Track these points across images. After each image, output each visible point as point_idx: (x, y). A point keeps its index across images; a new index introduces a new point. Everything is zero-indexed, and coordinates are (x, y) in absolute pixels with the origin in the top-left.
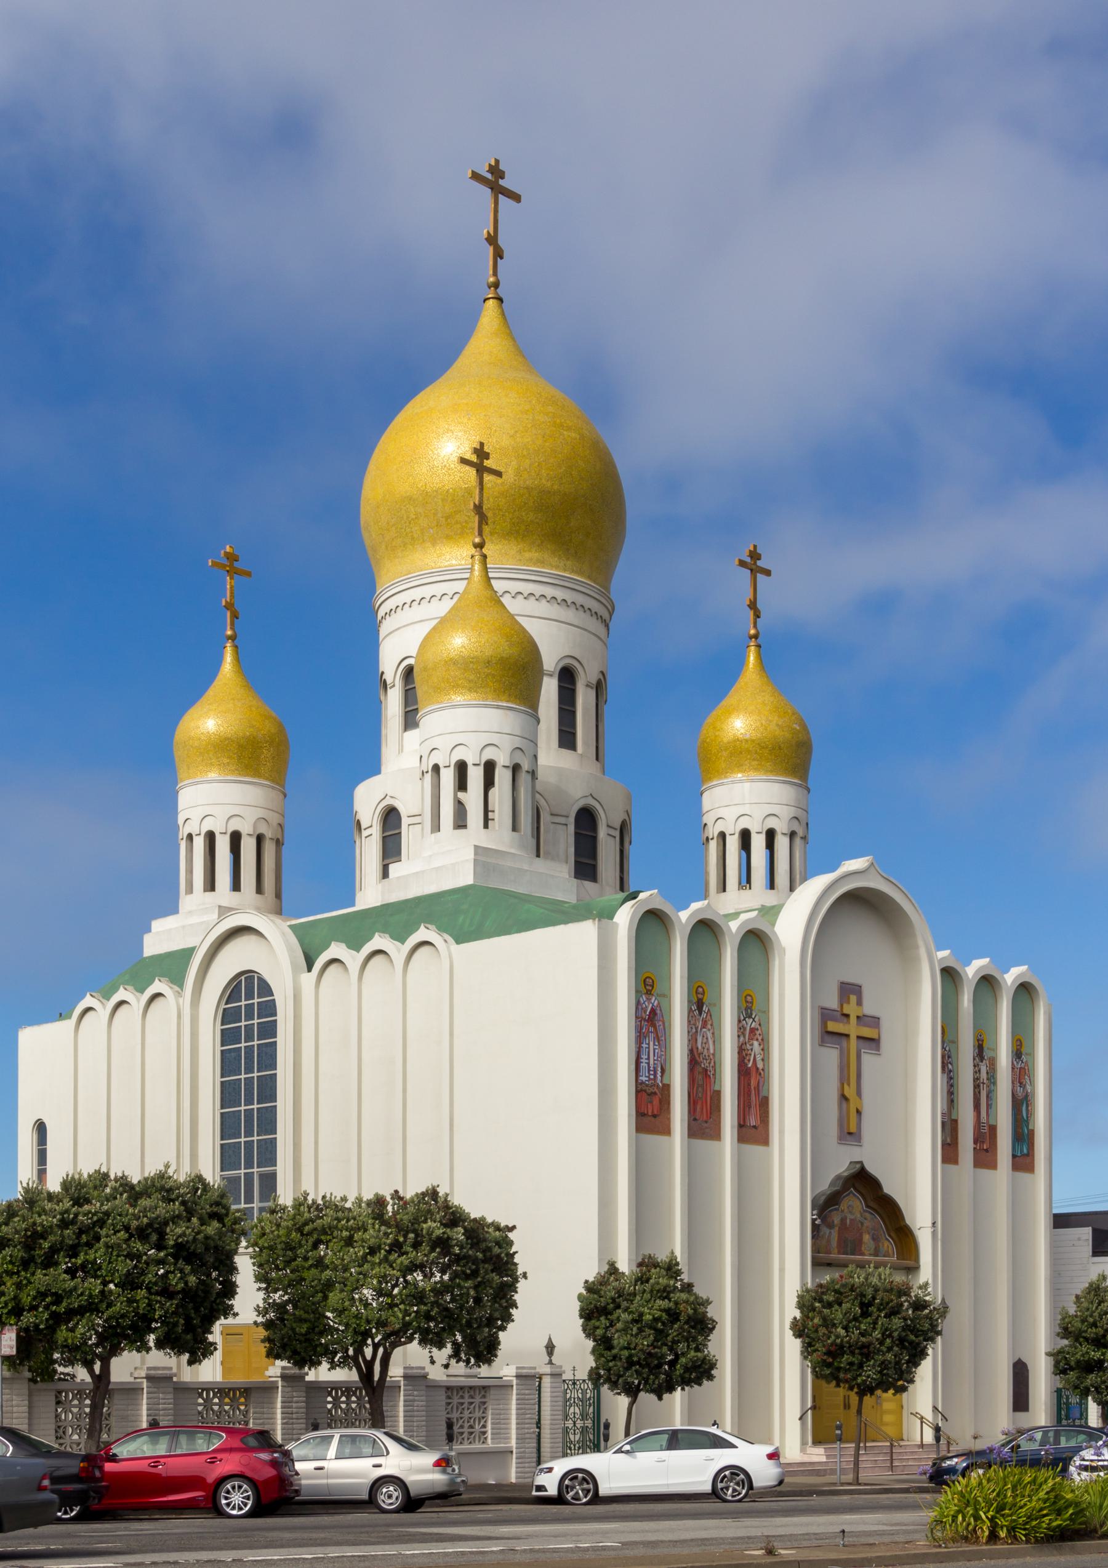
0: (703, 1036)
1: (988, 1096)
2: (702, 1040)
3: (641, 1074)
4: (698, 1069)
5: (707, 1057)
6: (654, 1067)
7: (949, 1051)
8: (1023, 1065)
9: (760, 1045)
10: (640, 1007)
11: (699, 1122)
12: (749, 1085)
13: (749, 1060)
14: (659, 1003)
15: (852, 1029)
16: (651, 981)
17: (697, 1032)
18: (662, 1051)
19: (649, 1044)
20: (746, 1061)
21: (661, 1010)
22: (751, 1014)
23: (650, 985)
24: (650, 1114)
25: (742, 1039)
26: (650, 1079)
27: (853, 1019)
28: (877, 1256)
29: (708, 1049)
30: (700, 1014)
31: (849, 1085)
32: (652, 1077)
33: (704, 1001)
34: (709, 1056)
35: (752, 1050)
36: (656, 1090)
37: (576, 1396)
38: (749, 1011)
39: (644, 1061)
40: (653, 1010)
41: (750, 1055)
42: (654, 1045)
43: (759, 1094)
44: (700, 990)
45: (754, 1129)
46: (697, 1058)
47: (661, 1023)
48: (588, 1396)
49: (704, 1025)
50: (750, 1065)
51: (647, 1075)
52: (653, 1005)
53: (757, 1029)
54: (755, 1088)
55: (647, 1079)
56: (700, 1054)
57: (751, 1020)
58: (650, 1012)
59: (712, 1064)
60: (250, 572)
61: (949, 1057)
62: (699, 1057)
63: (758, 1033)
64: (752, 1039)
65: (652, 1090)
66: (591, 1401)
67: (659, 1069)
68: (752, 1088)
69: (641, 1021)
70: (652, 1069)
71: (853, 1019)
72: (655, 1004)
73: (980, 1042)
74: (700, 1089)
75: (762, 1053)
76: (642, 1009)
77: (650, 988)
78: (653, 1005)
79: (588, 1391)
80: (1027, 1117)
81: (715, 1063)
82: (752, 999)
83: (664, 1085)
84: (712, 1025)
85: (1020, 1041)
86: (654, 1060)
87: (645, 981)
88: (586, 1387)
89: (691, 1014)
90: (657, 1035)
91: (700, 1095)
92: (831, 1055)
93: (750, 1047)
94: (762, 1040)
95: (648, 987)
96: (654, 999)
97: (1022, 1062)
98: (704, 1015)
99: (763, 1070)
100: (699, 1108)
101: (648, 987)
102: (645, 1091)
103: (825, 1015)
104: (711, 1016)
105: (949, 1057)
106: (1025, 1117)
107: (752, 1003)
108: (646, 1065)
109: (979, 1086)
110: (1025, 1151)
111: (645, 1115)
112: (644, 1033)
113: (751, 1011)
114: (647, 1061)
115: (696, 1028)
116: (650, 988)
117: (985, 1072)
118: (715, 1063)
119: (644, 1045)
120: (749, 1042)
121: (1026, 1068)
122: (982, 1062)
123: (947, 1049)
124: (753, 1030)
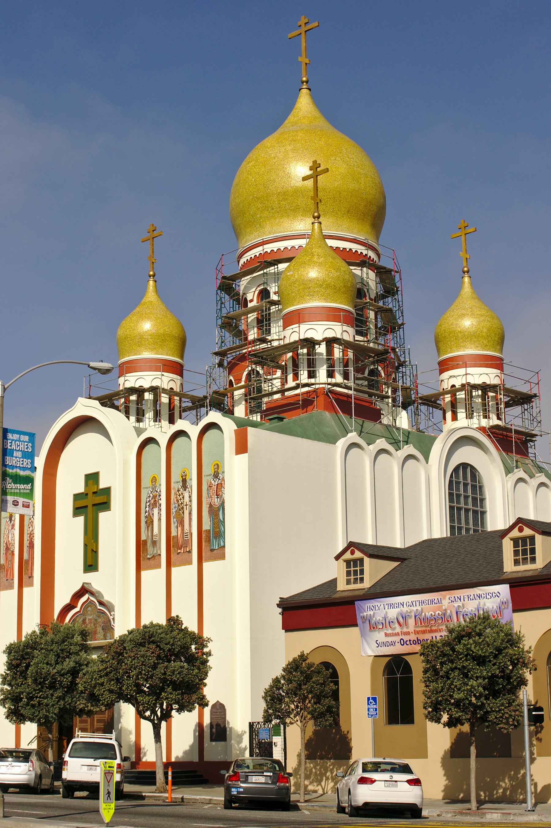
11: (9, 580)
25: (31, 528)
28: (106, 639)
30: (11, 522)
46: (9, 547)
74: (10, 563)
85: (217, 464)
89: (7, 524)
91: (10, 566)
97: (219, 479)
98: (12, 522)
100: (9, 574)
106: (222, 519)
109: (183, 508)
117: (188, 496)
121: (223, 482)
122: (185, 490)
123: (158, 491)
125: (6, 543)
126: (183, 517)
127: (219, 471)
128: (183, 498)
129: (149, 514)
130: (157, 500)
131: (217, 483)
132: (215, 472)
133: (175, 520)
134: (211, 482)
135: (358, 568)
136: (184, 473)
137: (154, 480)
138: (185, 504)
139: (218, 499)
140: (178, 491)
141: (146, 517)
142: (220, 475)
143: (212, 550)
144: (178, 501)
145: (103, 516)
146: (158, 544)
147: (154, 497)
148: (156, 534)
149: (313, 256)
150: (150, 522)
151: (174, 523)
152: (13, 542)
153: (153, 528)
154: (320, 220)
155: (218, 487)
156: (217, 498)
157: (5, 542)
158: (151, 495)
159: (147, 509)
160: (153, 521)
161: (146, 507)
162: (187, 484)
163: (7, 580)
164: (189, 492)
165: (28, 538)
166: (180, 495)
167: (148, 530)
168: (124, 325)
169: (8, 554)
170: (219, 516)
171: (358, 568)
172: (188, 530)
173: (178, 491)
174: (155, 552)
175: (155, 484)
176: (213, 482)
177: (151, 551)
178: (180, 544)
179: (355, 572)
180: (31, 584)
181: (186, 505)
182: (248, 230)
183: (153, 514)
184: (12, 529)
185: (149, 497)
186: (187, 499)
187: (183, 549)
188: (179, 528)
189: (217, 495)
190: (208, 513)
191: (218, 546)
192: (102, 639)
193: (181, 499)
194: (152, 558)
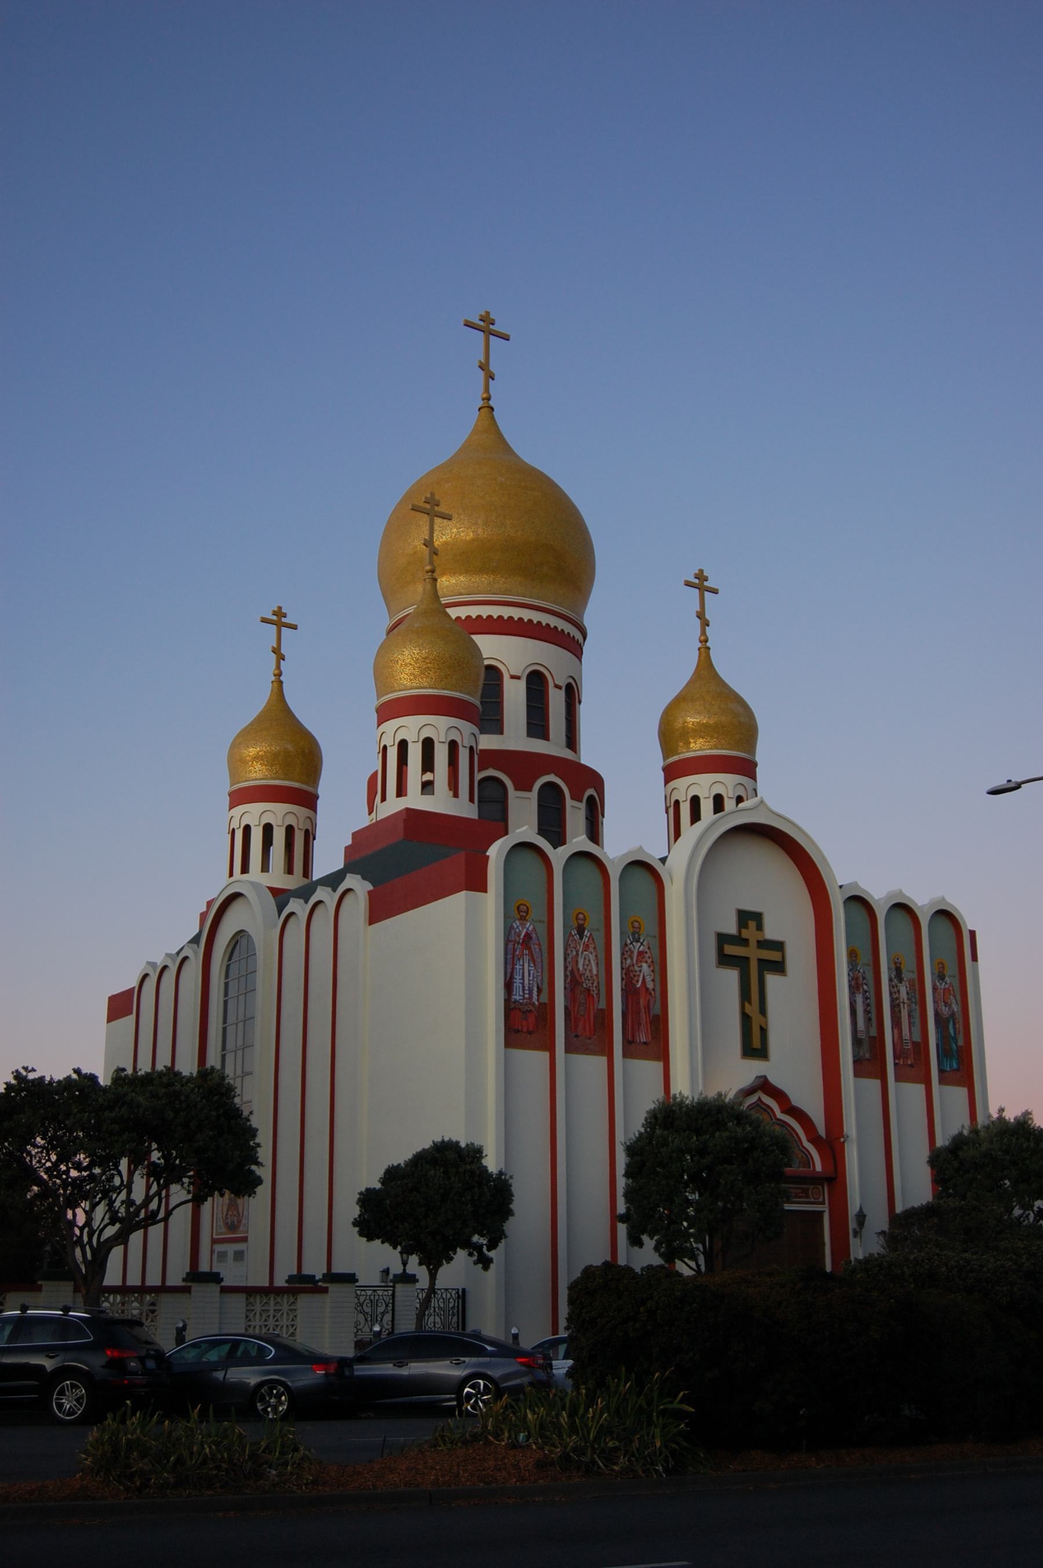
0: (585, 959)
1: (909, 1015)
2: (584, 962)
3: (514, 993)
5: (590, 978)
6: (529, 987)
7: (864, 972)
9: (649, 967)
10: (513, 932)
12: (638, 1003)
13: (638, 981)
14: (534, 928)
15: (753, 953)
16: (525, 908)
17: (577, 954)
18: (537, 972)
19: (523, 966)
20: (634, 981)
21: (536, 934)
22: (639, 939)
23: (525, 912)
24: (525, 1030)
25: (629, 961)
26: (524, 998)
27: (753, 943)
29: (591, 971)
30: (581, 938)
31: (750, 1003)
32: (527, 996)
33: (585, 926)
34: (591, 977)
35: (640, 971)
36: (531, 1008)
37: (437, 1305)
38: (637, 936)
39: (518, 981)
40: (528, 936)
41: (639, 976)
42: (529, 966)
43: (649, 1012)
45: (645, 1046)
46: (578, 978)
47: (536, 946)
48: (451, 1305)
49: (586, 947)
50: (639, 986)
51: (521, 994)
52: (528, 929)
53: (646, 953)
54: (645, 1008)
55: (521, 998)
56: (581, 975)
57: (639, 944)
58: (525, 936)
59: (595, 984)
60: (297, 626)
62: (581, 978)
63: (647, 956)
64: (641, 962)
65: (526, 1008)
66: (455, 1311)
67: (535, 989)
68: (642, 1006)
69: (514, 945)
70: (527, 988)
71: (753, 943)
72: (530, 929)
73: (898, 965)
75: (652, 974)
76: (515, 932)
77: (525, 914)
78: (528, 929)
79: (451, 1300)
80: (955, 1034)
81: (598, 983)
82: (640, 924)
83: (540, 1004)
84: (594, 948)
85: (942, 964)
86: (529, 980)
87: (518, 908)
88: (449, 1296)
90: (532, 957)
92: (732, 976)
93: (638, 969)
94: (652, 962)
95: (521, 914)
96: (528, 924)
97: (946, 983)
99: (653, 990)
100: (581, 1025)
101: (521, 914)
102: (519, 1009)
103: (722, 939)
104: (593, 939)
105: (864, 979)
107: (640, 928)
108: (521, 985)
109: (899, 1005)
110: (955, 1066)
111: (519, 1031)
112: (518, 955)
113: (639, 935)
114: (521, 981)
115: (577, 952)
116: (525, 914)
118: (598, 983)
119: (518, 967)
120: (637, 964)
121: (951, 988)
122: (901, 983)
123: (861, 971)
124: (640, 953)
125: (572, 972)
126: (900, 1018)
127: (945, 972)
128: (899, 991)
130: (860, 983)
131: (943, 987)
132: (940, 972)
136: (898, 959)
138: (901, 1001)
139: (947, 1008)
142: (947, 978)
145: (772, 980)
148: (861, 1029)
156: (946, 1006)
157: (570, 968)
162: (903, 975)
164: (907, 987)
165: (624, 976)
166: (893, 987)
172: (908, 1036)
174: (861, 1054)
175: (856, 960)
187: (902, 1060)
188: (896, 1031)
189: (944, 1002)
191: (950, 1068)
193: (895, 993)
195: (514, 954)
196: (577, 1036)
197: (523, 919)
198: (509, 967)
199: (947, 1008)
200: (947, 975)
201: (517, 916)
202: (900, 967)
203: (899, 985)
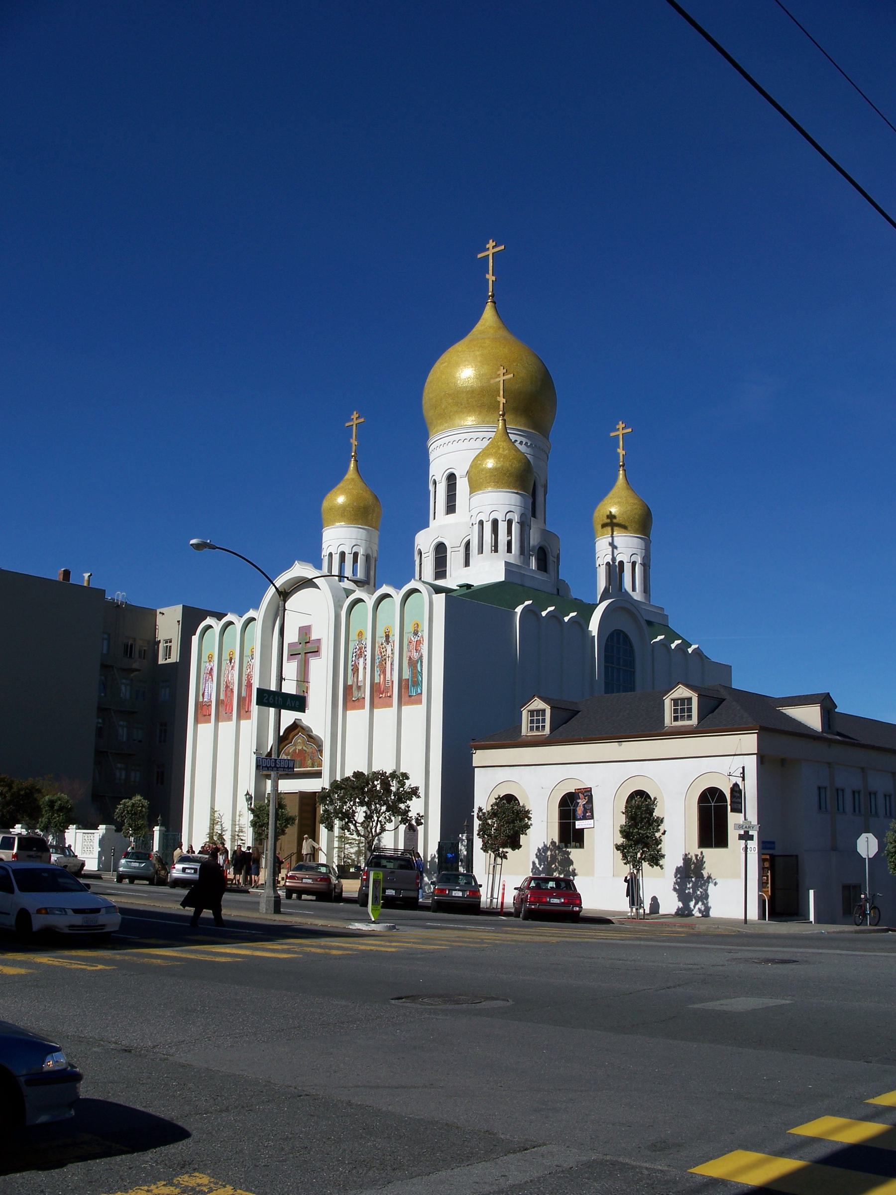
1: (391, 664)
4: (229, 689)
8: (419, 638)
11: (228, 714)
25: (249, 670)
30: (231, 664)
44: (211, 656)
61: (365, 648)
85: (417, 624)
97: (418, 636)
98: (232, 664)
100: (228, 708)
105: (365, 648)
106: (420, 670)
109: (385, 659)
115: (229, 671)
117: (391, 649)
119: (207, 685)
121: (422, 639)
122: (388, 644)
123: (364, 644)
125: (226, 682)
128: (386, 651)
129: (355, 663)
130: (362, 651)
131: (416, 640)
133: (378, 669)
134: (411, 639)
135: (540, 718)
137: (360, 634)
138: (387, 656)
139: (417, 653)
140: (382, 644)
141: (352, 665)
142: (419, 633)
143: (410, 696)
144: (381, 653)
146: (362, 689)
147: (360, 649)
149: (499, 448)
150: (356, 670)
151: (377, 672)
152: (232, 681)
153: (358, 675)
154: (505, 418)
155: (418, 643)
158: (358, 647)
159: (354, 658)
160: (358, 669)
161: (353, 657)
163: (226, 713)
166: (383, 648)
167: (354, 676)
168: (330, 497)
169: (228, 691)
170: (417, 667)
171: (540, 718)
172: (390, 678)
173: (382, 644)
174: (360, 695)
176: (413, 638)
177: (356, 694)
178: (382, 689)
179: (538, 721)
180: (249, 718)
181: (389, 657)
182: (439, 422)
183: (359, 663)
184: (232, 670)
185: (356, 648)
186: (389, 652)
187: (384, 694)
188: (382, 676)
189: (416, 650)
190: (407, 664)
191: (416, 693)
192: (310, 767)
193: (384, 652)
194: (356, 700)
195: (206, 680)
196: (226, 713)
197: (210, 661)
198: (204, 686)
199: (417, 653)
200: (419, 631)
201: (208, 661)
202: (388, 634)
203: (387, 646)
